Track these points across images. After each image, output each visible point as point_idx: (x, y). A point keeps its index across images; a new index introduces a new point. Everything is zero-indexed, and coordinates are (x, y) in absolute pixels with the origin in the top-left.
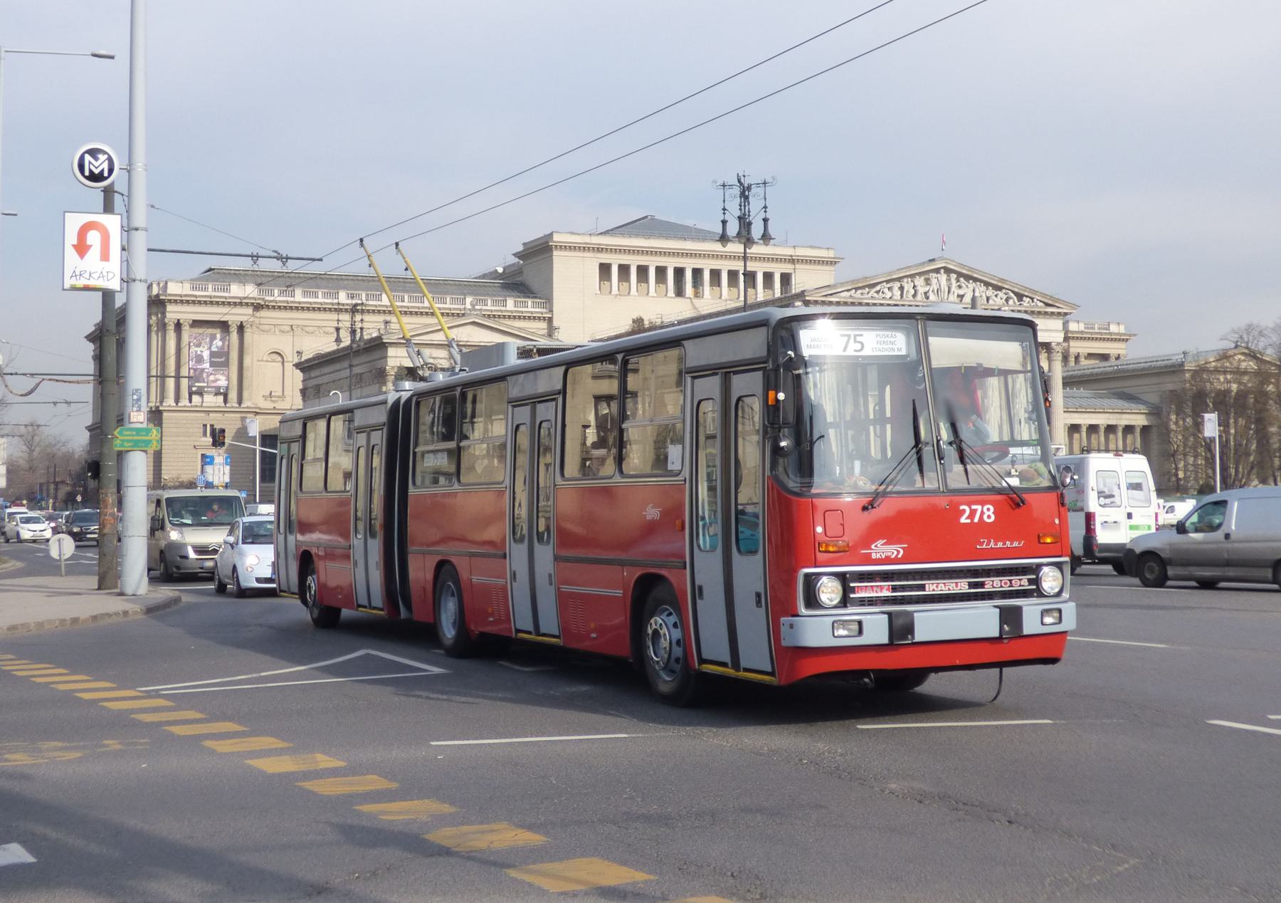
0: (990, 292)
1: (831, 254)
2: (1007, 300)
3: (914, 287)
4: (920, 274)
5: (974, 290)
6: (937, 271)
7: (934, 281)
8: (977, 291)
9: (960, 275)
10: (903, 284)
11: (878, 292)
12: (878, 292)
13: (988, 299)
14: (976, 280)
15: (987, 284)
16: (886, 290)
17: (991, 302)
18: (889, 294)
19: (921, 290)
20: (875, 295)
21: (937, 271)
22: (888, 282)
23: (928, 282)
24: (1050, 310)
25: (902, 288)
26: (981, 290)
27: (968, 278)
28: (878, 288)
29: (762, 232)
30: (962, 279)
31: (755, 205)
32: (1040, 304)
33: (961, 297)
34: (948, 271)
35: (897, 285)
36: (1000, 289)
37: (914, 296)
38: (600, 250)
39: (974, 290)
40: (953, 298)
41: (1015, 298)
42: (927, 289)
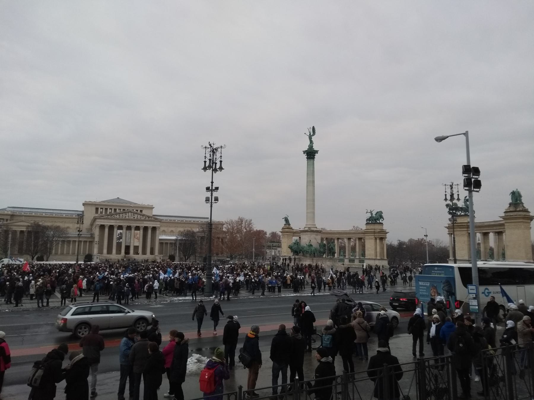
3: (123, 215)
5: (137, 216)
6: (129, 212)
7: (128, 214)
10: (120, 215)
18: (116, 217)
19: (124, 216)
21: (129, 212)
23: (126, 214)
25: (120, 215)
28: (114, 215)
29: (445, 198)
34: (131, 212)
35: (118, 215)
39: (137, 216)
40: (132, 218)
42: (125, 216)
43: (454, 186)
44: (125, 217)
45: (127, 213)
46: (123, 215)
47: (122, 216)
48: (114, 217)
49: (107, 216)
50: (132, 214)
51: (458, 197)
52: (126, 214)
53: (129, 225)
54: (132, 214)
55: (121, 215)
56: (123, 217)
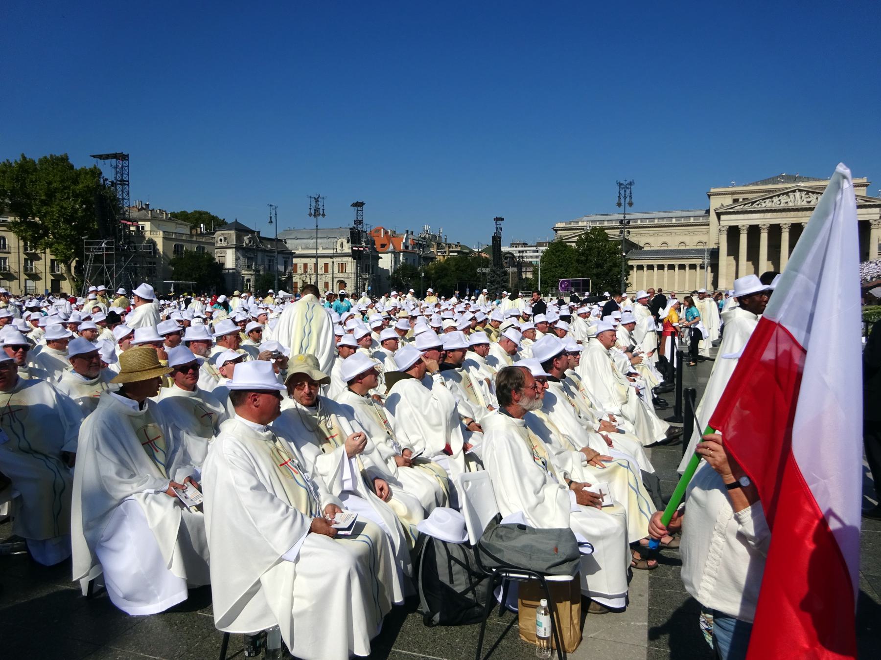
1: (864, 180)
4: (783, 194)
5: (817, 198)
6: (794, 191)
8: (819, 198)
9: (808, 192)
11: (758, 205)
12: (758, 205)
14: (818, 193)
16: (763, 203)
18: (764, 205)
19: (783, 201)
20: (757, 206)
21: (794, 191)
22: (763, 199)
24: (868, 203)
25: (773, 202)
27: (813, 193)
28: (757, 203)
30: (810, 194)
31: (321, 205)
32: (860, 201)
33: (809, 202)
34: (800, 191)
35: (767, 201)
37: (780, 204)
38: (733, 193)
39: (817, 198)
43: (319, 200)
44: (787, 203)
47: (779, 202)
48: (760, 206)
49: (742, 207)
50: (803, 195)
51: (323, 212)
53: (795, 221)
54: (803, 195)
55: (776, 199)
56: (780, 204)
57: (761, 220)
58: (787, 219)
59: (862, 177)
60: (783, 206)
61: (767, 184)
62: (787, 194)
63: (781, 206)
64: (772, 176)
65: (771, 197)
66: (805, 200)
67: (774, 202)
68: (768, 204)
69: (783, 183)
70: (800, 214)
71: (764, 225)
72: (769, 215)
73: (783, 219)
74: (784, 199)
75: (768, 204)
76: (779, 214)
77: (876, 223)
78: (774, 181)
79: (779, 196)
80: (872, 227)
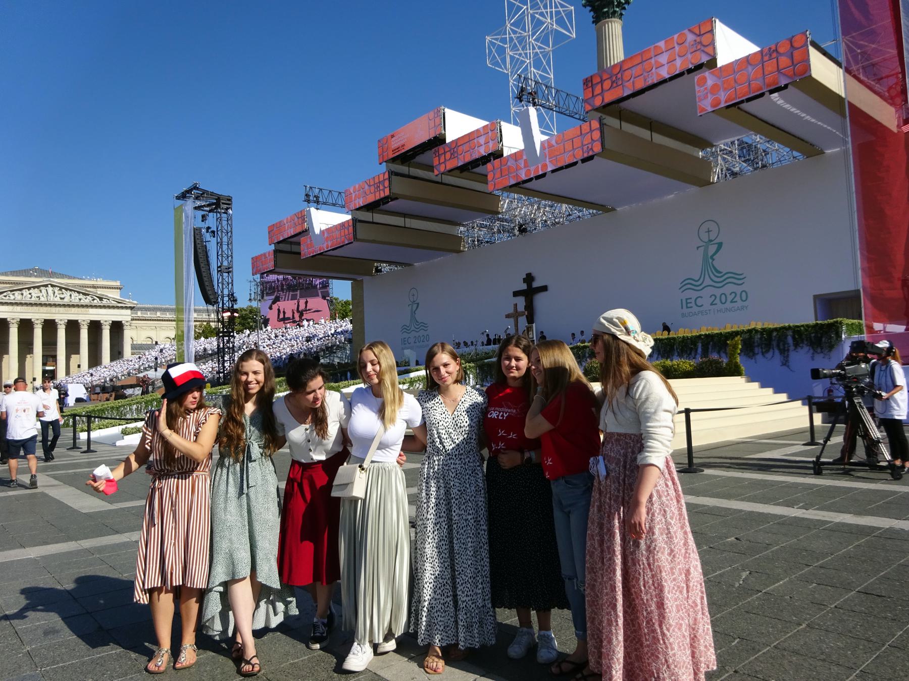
0: (81, 296)
1: (118, 284)
2: (93, 300)
4: (34, 288)
5: (71, 295)
6: (46, 286)
9: (61, 288)
12: (5, 296)
13: (80, 299)
14: (71, 290)
15: (79, 292)
16: (11, 295)
17: (82, 301)
18: (12, 297)
20: (4, 298)
21: (46, 286)
22: (11, 291)
24: (120, 305)
25: (22, 294)
26: (74, 295)
27: (66, 289)
28: (5, 294)
30: (63, 290)
34: (52, 286)
35: (17, 293)
36: (88, 295)
37: (31, 298)
39: (71, 295)
41: (98, 299)
45: (42, 288)
46: (30, 294)
47: (30, 296)
48: (7, 298)
52: (41, 291)
54: (56, 291)
55: (26, 292)
56: (31, 298)
57: (10, 314)
58: (39, 315)
59: (115, 280)
60: (34, 300)
61: (17, 276)
62: (38, 287)
63: (32, 299)
64: (23, 269)
65: (20, 290)
66: (58, 296)
67: (24, 295)
68: (17, 296)
69: (36, 276)
70: (53, 309)
71: (13, 319)
72: (19, 308)
73: (36, 314)
74: (35, 292)
75: (17, 296)
76: (30, 309)
77: (128, 324)
78: (25, 273)
79: (29, 289)
80: (125, 327)
